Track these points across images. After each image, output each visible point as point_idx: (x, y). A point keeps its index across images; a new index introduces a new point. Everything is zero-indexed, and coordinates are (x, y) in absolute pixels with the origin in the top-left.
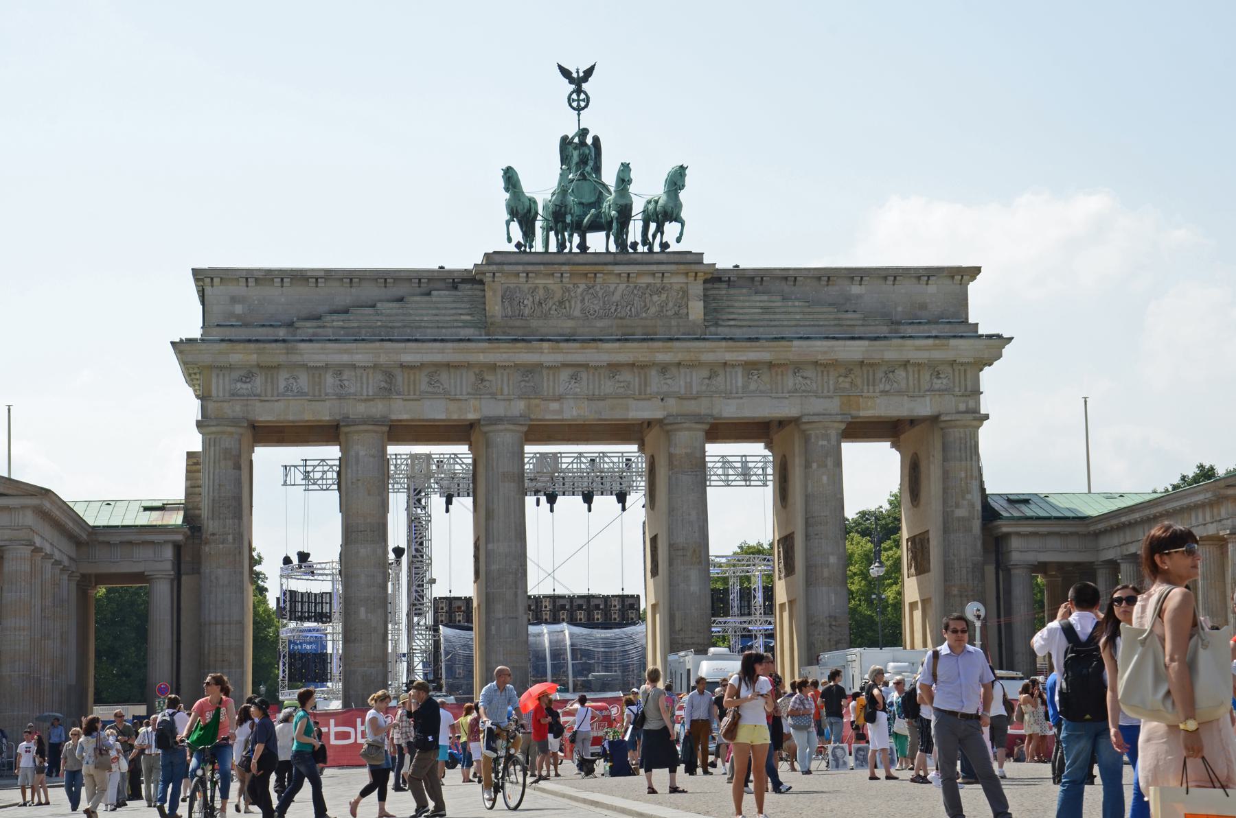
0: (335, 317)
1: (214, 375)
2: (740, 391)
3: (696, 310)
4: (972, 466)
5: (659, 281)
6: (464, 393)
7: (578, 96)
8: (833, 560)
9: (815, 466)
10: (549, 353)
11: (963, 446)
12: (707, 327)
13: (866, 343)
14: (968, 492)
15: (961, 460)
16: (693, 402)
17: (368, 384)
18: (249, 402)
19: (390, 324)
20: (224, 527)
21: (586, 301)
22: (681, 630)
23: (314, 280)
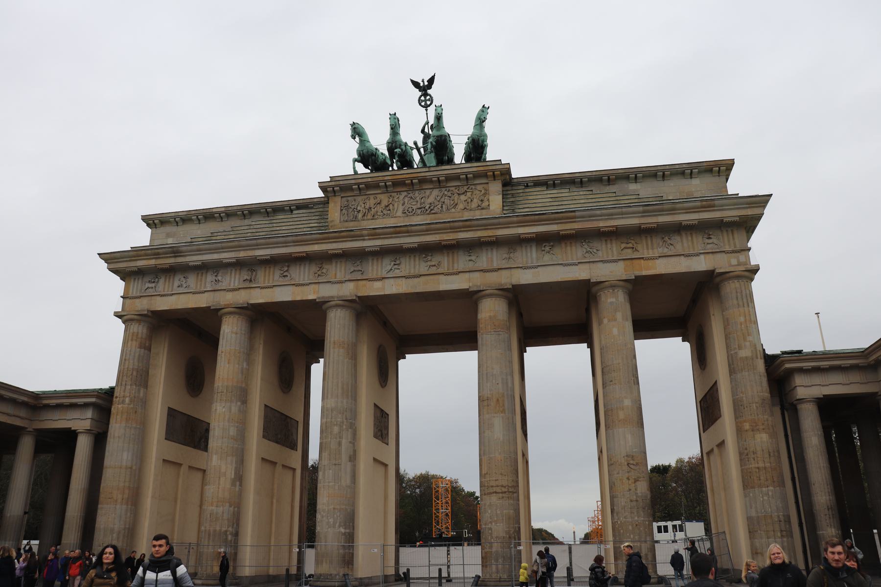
0: (219, 234)
1: (132, 280)
2: (535, 262)
3: (495, 202)
4: (749, 312)
6: (306, 279)
7: (425, 97)
8: (627, 402)
9: (605, 321)
10: (370, 239)
11: (739, 294)
12: (504, 214)
13: (641, 209)
14: (749, 335)
15: (739, 306)
16: (495, 274)
17: (235, 278)
18: (153, 298)
19: (257, 234)
20: (124, 391)
21: (406, 204)
22: (487, 473)
23: (218, 215)
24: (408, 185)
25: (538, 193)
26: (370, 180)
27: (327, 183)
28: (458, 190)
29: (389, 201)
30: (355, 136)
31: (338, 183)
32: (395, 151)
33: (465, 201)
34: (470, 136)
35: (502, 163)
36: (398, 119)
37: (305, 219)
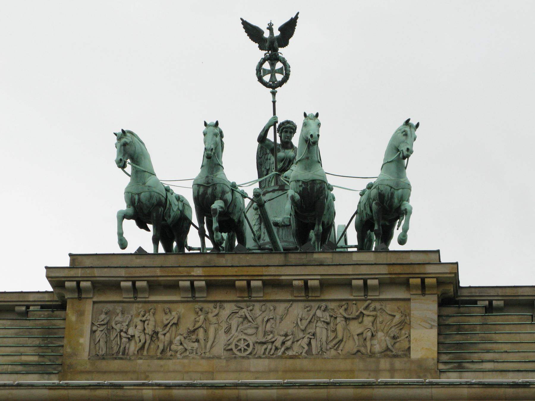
5: (360, 295)
7: (273, 65)
12: (441, 372)
24: (241, 290)
25: (514, 329)
26: (158, 272)
27: (66, 270)
28: (346, 310)
29: (196, 322)
30: (125, 162)
31: (88, 272)
32: (214, 206)
33: (358, 335)
34: (373, 181)
35: (443, 261)
36: (221, 133)
37: (10, 342)
